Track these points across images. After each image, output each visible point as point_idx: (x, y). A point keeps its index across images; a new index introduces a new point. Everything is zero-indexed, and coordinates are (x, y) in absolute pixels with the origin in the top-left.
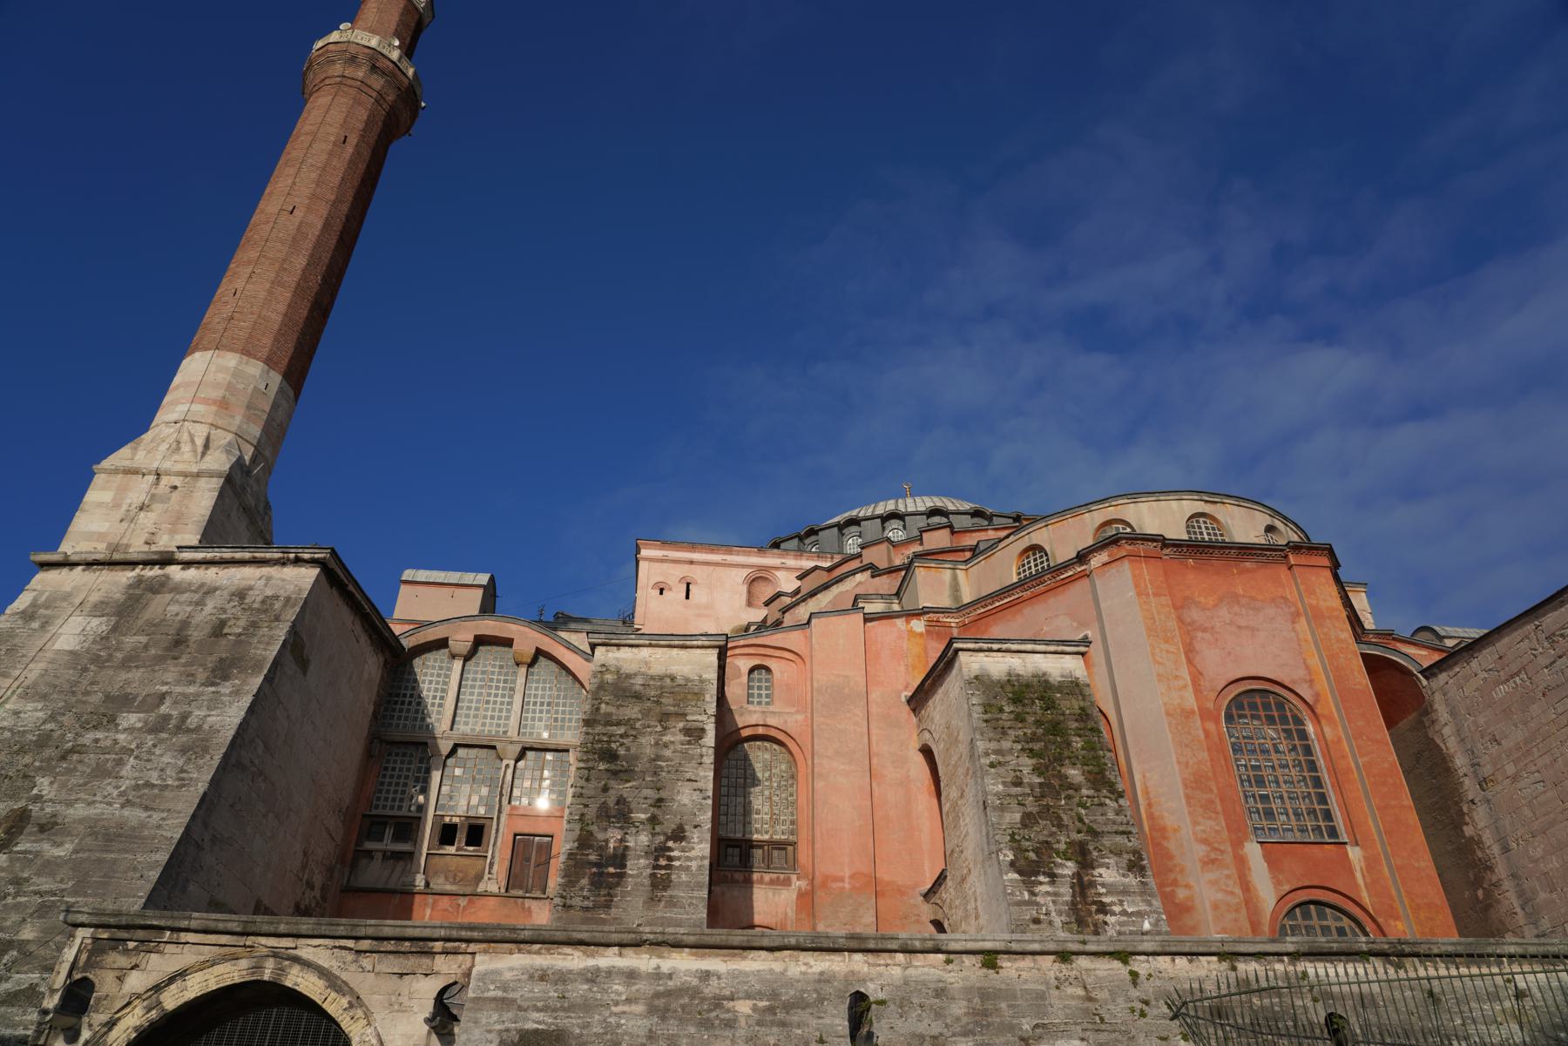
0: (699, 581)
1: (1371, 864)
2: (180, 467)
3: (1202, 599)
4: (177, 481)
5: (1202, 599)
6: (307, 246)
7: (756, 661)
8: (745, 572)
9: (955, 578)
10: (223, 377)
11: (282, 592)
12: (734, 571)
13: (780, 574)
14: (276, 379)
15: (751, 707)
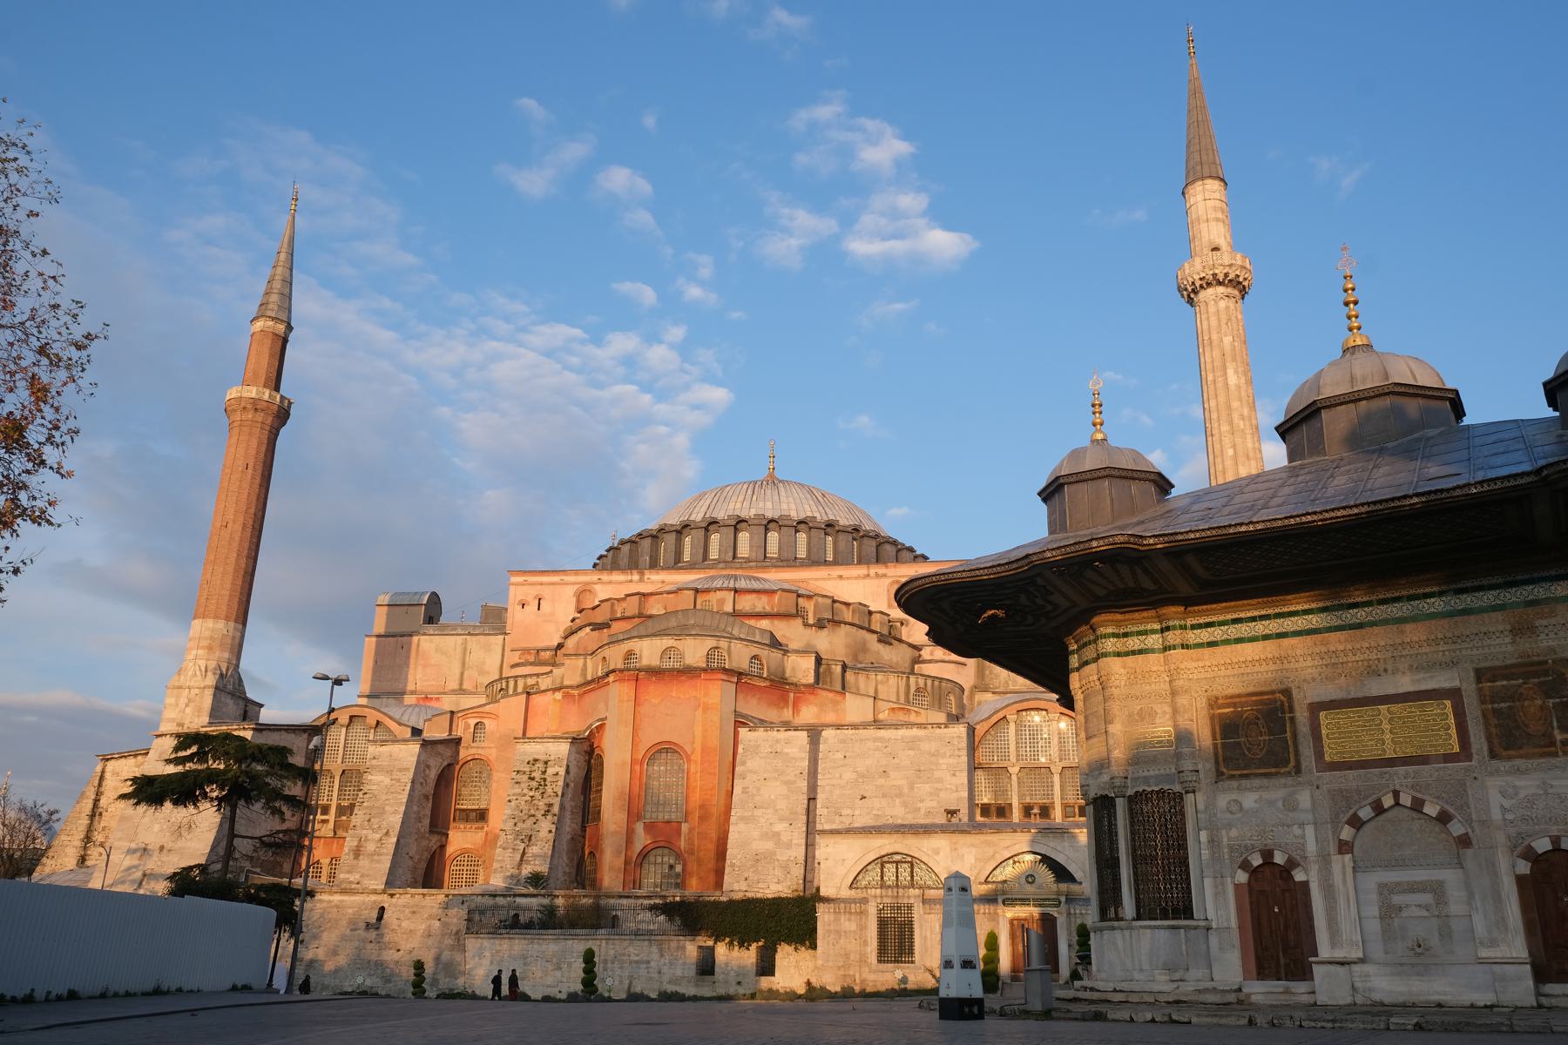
0: (547, 597)
1: (691, 830)
2: (196, 684)
3: (653, 701)
4: (197, 691)
5: (653, 701)
6: (235, 545)
7: (479, 720)
8: (576, 587)
9: (585, 665)
10: (208, 634)
11: (188, 837)
12: (569, 587)
13: (597, 587)
14: (232, 624)
15: (473, 745)
